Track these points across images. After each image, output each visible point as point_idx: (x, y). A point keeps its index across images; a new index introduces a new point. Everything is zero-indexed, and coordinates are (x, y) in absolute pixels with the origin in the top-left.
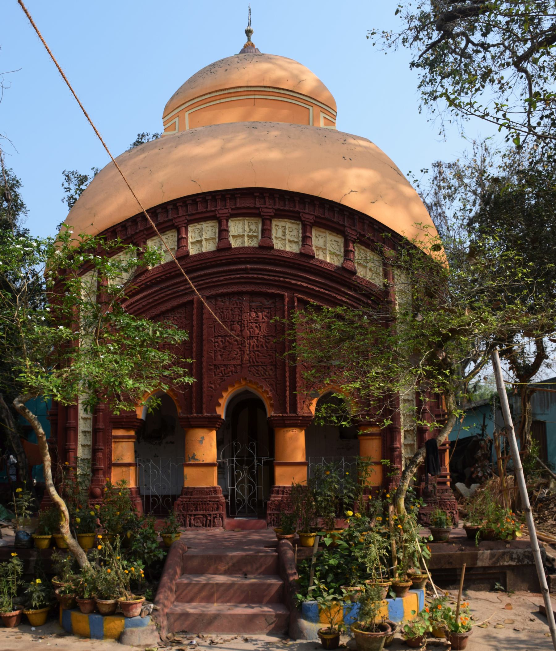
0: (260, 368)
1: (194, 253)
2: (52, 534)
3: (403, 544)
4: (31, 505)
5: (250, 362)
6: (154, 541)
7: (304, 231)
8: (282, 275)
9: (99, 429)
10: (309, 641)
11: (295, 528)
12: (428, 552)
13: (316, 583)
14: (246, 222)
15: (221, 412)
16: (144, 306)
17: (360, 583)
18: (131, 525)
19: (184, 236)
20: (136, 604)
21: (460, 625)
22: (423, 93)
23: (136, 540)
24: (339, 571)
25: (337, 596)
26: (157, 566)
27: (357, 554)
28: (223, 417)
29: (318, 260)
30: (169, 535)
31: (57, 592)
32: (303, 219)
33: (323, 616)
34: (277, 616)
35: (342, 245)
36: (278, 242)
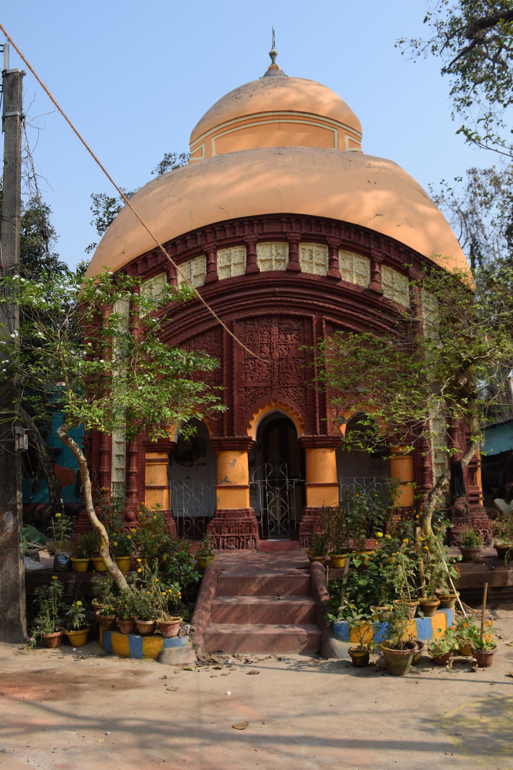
0: (290, 390)
1: (223, 278)
2: (90, 557)
3: (430, 565)
4: (69, 529)
5: (279, 384)
6: (189, 564)
7: (331, 254)
8: (309, 298)
10: (340, 660)
11: (326, 550)
12: (456, 572)
13: (346, 603)
14: (273, 247)
15: (252, 434)
16: (175, 331)
17: (389, 603)
18: (165, 548)
19: (213, 261)
20: (174, 624)
21: (485, 642)
22: (455, 100)
23: (173, 563)
24: (369, 591)
25: (366, 615)
27: (385, 575)
28: (254, 439)
29: (345, 282)
30: (204, 558)
31: (97, 613)
32: (329, 243)
33: (354, 636)
34: (309, 635)
35: (369, 267)
36: (305, 265)
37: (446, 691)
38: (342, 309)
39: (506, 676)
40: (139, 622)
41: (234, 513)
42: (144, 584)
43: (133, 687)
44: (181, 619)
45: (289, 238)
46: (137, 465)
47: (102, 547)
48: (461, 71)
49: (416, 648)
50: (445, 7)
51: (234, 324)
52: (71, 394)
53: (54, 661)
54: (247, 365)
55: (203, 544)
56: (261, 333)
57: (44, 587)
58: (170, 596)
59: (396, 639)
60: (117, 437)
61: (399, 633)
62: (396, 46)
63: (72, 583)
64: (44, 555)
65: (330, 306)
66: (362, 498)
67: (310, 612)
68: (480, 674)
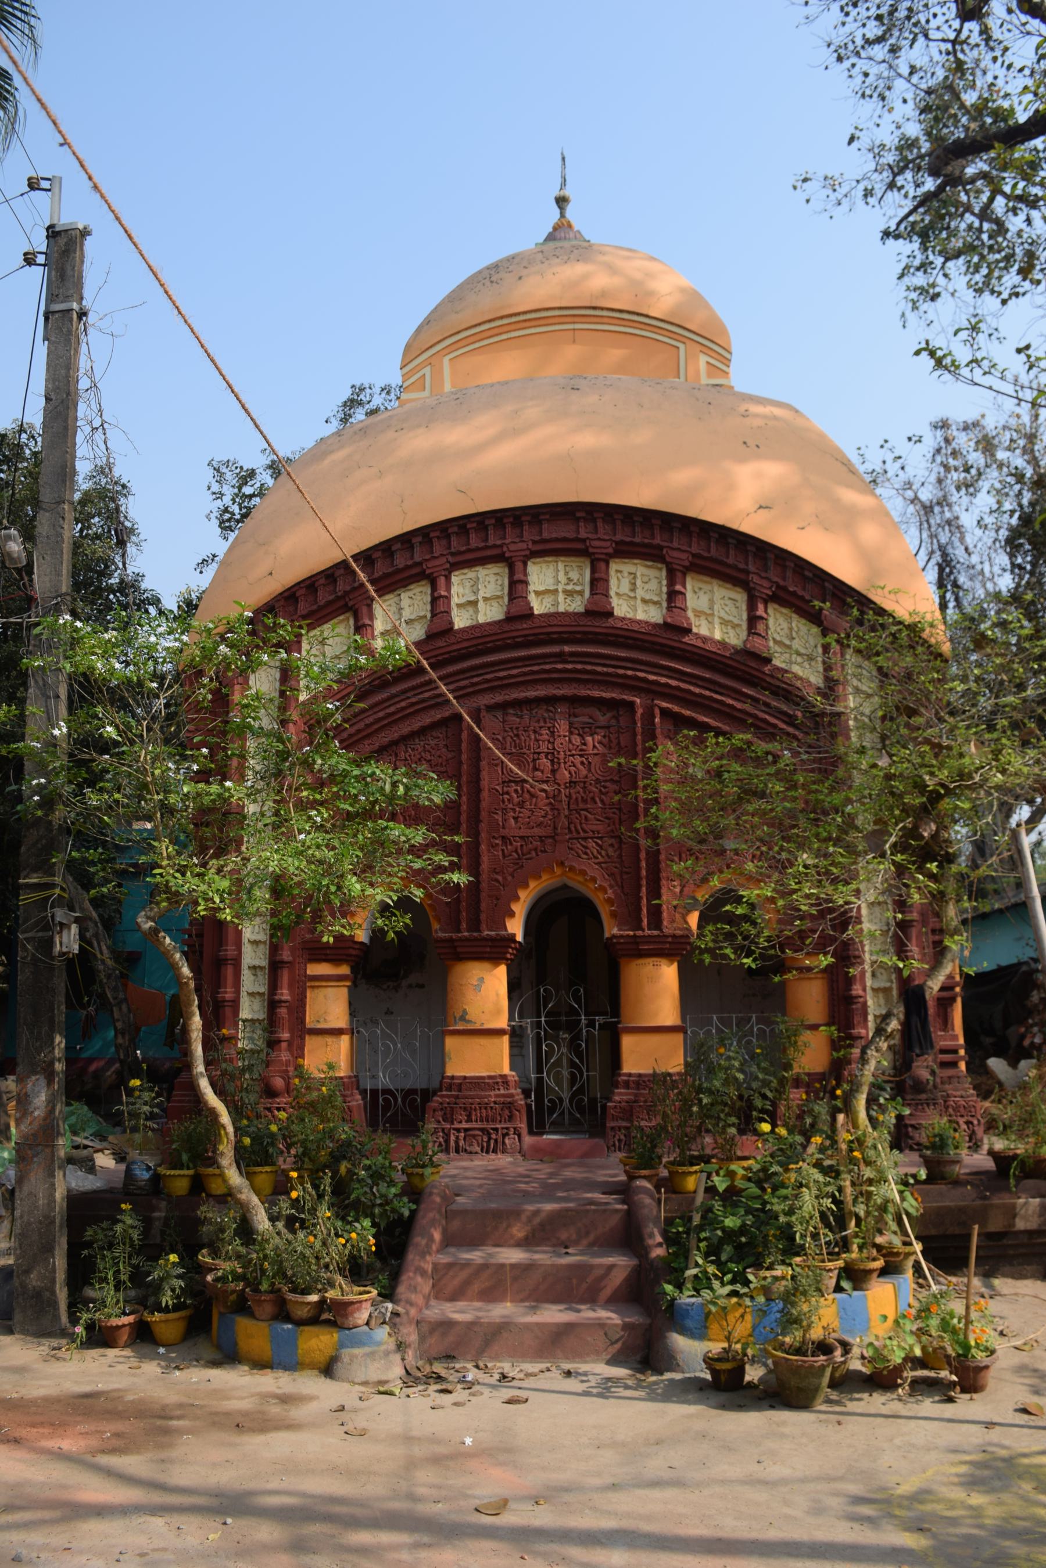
0: (591, 844)
1: (462, 626)
2: (195, 1167)
3: (865, 1188)
4: (156, 1110)
5: (570, 831)
6: (392, 1183)
7: (671, 581)
8: (629, 665)
9: (283, 962)
11: (660, 1158)
12: (914, 1203)
13: (698, 1264)
14: (561, 566)
15: (516, 927)
16: (368, 726)
17: (783, 1263)
18: (343, 1151)
19: (443, 593)
20: (361, 1302)
21: (973, 1343)
22: (908, 289)
23: (359, 1181)
24: (743, 1239)
25: (738, 1287)
26: (398, 1231)
27: (777, 1208)
28: (520, 938)
29: (698, 636)
30: (420, 1170)
31: (209, 1278)
32: (668, 559)
33: (714, 1328)
34: (626, 1327)
35: (744, 607)
36: (621, 602)
37: (897, 1441)
38: (692, 688)
39: (1016, 1410)
40: (291, 1296)
41: (478, 1083)
42: (303, 1222)
43: (277, 1428)
44: (375, 1292)
45: (591, 550)
46: (291, 987)
47: (221, 1148)
48: (920, 236)
49: (838, 1352)
50: (888, 118)
51: (483, 713)
52: (165, 847)
53: (121, 1373)
54: (507, 793)
55: (417, 1142)
56: (535, 732)
57: (105, 1225)
58: (353, 1246)
59: (798, 1334)
60: (252, 931)
61: (805, 1323)
62: (795, 188)
63: (159, 1219)
64: (105, 1160)
65: (670, 681)
66: (730, 1056)
67: (627, 1280)
68: (965, 1406)
